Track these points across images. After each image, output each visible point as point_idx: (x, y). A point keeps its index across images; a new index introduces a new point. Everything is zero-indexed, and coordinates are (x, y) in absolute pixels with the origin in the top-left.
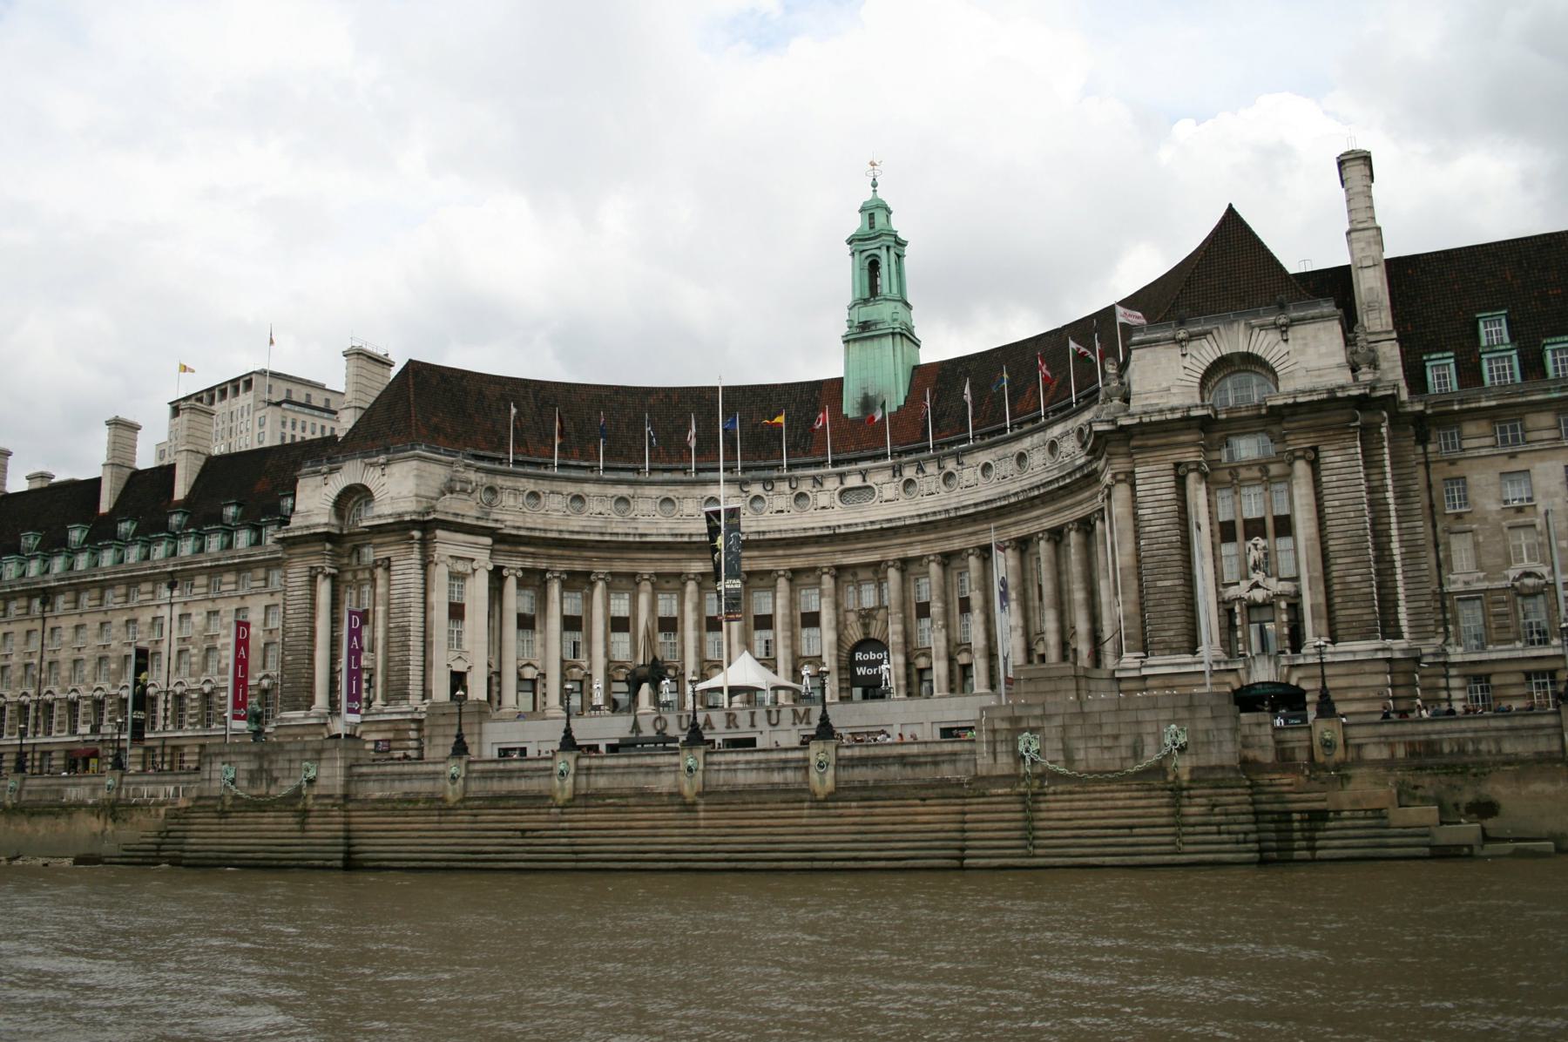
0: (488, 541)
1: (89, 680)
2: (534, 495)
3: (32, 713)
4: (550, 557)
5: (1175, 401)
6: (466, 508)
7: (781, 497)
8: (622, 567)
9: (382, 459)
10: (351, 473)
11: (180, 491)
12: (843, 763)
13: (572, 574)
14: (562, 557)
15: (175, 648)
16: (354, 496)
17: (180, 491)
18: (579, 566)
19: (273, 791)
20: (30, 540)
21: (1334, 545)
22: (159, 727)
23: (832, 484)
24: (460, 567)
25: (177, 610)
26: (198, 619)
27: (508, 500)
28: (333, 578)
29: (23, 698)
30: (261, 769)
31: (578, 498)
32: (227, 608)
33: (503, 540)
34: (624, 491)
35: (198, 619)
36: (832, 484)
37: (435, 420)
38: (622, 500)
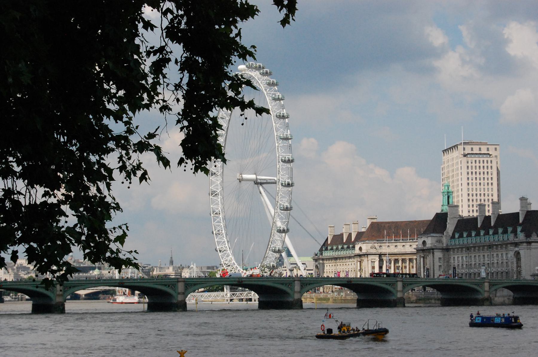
0: (378, 256)
2: (388, 246)
4: (391, 256)
6: (373, 251)
8: (403, 257)
9: (362, 243)
13: (395, 259)
14: (393, 256)
16: (360, 249)
18: (396, 258)
20: (335, 248)
24: (373, 260)
27: (383, 247)
28: (360, 261)
31: (396, 246)
33: (380, 255)
34: (404, 244)
37: (373, 234)
38: (403, 246)
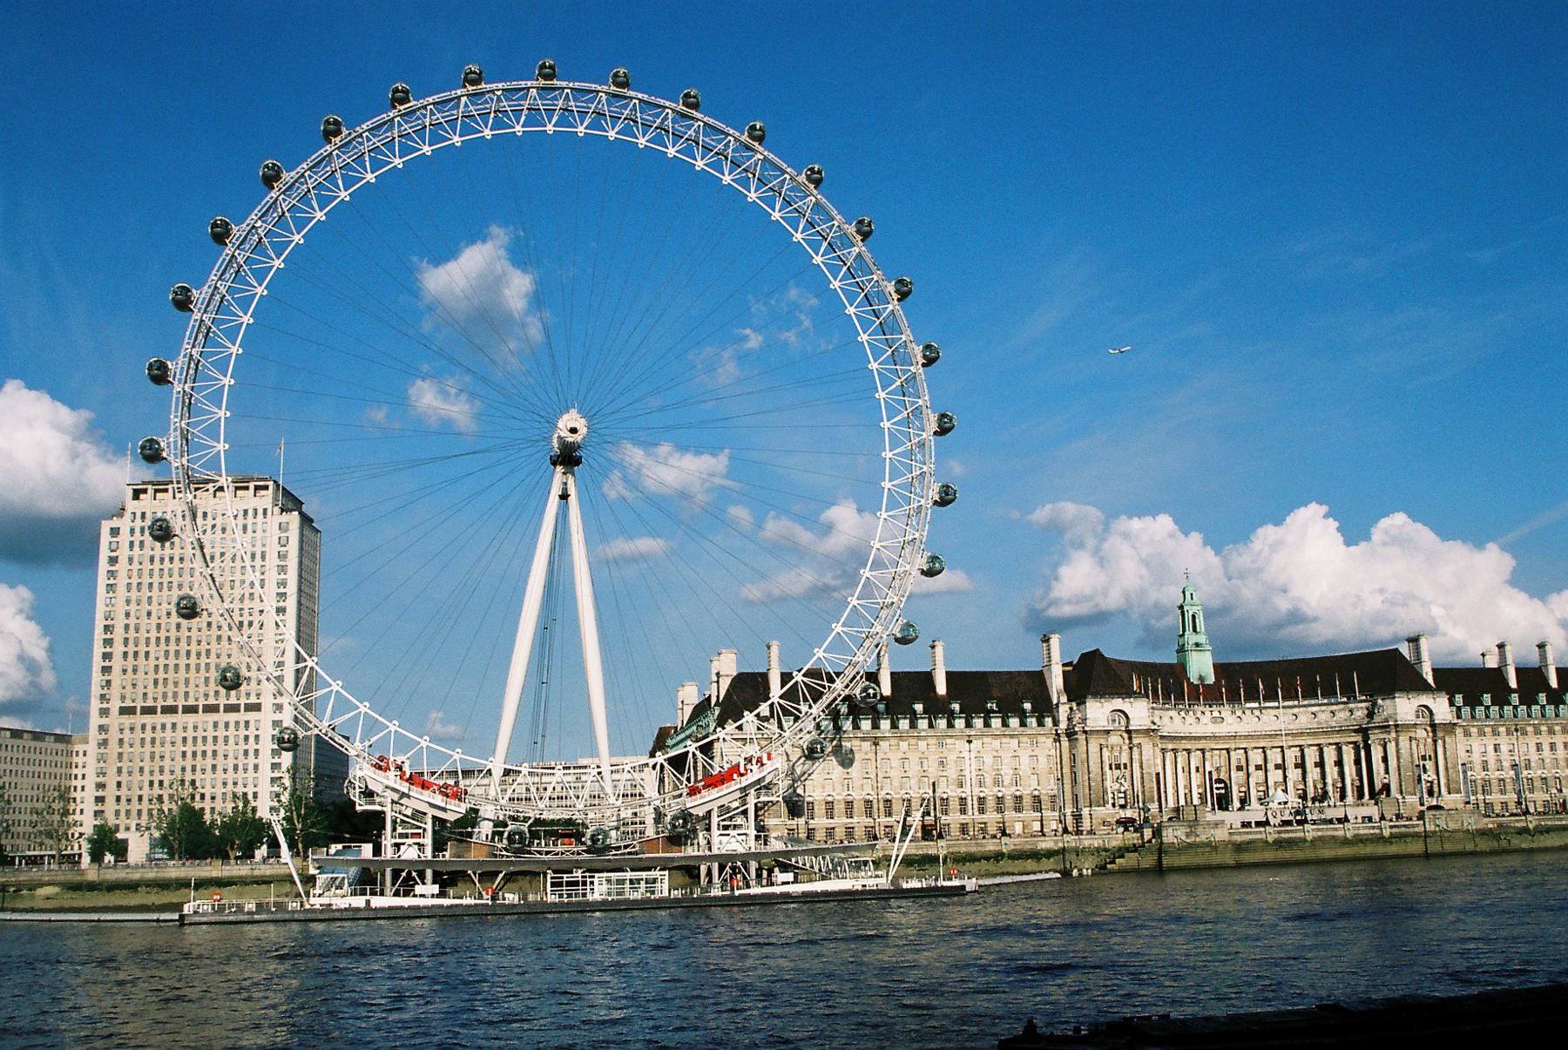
1: (917, 790)
3: (875, 806)
5: (1409, 718)
7: (1190, 718)
10: (1118, 703)
11: (941, 688)
12: (1391, 827)
15: (974, 774)
17: (941, 688)
19: (1198, 839)
21: (1449, 765)
22: (970, 812)
23: (1208, 713)
25: (973, 755)
26: (989, 760)
29: (868, 797)
30: (1191, 831)
32: (1007, 757)
35: (989, 760)
36: (1208, 713)
